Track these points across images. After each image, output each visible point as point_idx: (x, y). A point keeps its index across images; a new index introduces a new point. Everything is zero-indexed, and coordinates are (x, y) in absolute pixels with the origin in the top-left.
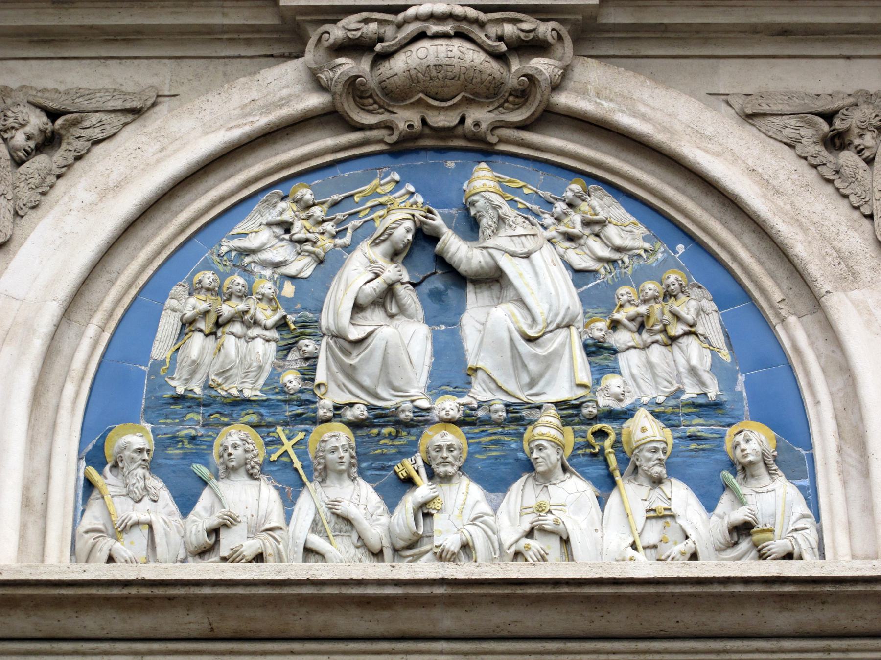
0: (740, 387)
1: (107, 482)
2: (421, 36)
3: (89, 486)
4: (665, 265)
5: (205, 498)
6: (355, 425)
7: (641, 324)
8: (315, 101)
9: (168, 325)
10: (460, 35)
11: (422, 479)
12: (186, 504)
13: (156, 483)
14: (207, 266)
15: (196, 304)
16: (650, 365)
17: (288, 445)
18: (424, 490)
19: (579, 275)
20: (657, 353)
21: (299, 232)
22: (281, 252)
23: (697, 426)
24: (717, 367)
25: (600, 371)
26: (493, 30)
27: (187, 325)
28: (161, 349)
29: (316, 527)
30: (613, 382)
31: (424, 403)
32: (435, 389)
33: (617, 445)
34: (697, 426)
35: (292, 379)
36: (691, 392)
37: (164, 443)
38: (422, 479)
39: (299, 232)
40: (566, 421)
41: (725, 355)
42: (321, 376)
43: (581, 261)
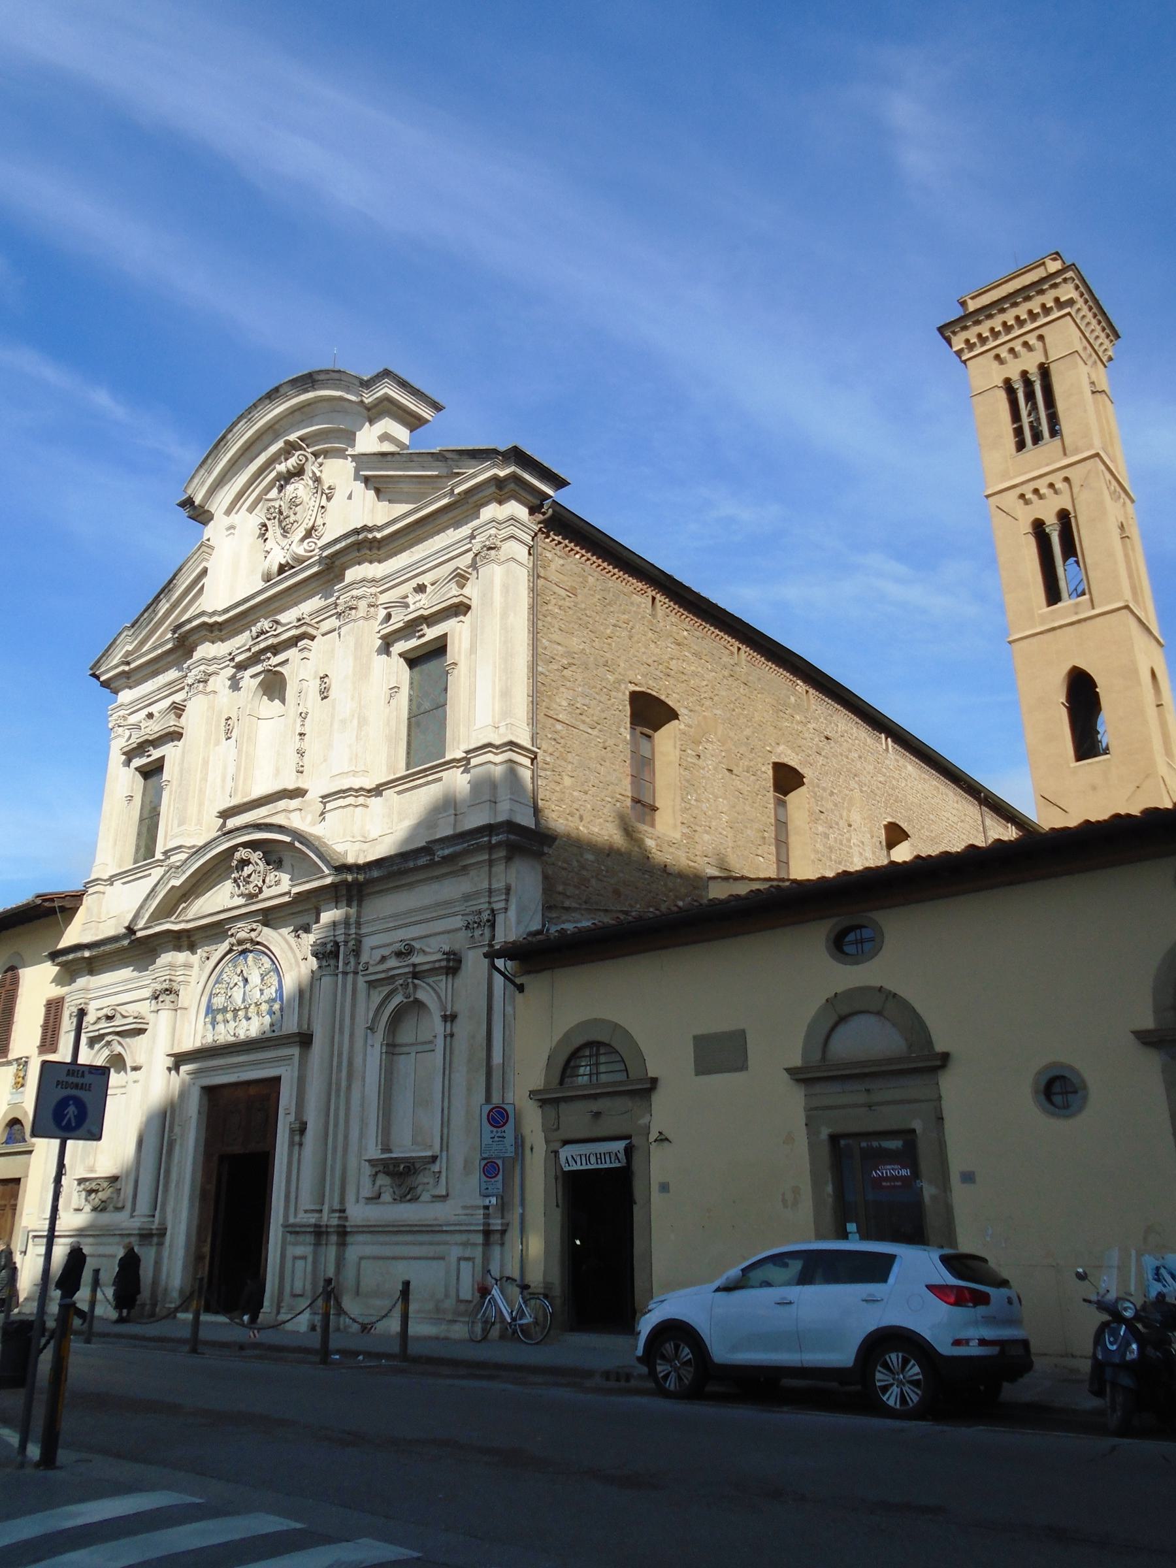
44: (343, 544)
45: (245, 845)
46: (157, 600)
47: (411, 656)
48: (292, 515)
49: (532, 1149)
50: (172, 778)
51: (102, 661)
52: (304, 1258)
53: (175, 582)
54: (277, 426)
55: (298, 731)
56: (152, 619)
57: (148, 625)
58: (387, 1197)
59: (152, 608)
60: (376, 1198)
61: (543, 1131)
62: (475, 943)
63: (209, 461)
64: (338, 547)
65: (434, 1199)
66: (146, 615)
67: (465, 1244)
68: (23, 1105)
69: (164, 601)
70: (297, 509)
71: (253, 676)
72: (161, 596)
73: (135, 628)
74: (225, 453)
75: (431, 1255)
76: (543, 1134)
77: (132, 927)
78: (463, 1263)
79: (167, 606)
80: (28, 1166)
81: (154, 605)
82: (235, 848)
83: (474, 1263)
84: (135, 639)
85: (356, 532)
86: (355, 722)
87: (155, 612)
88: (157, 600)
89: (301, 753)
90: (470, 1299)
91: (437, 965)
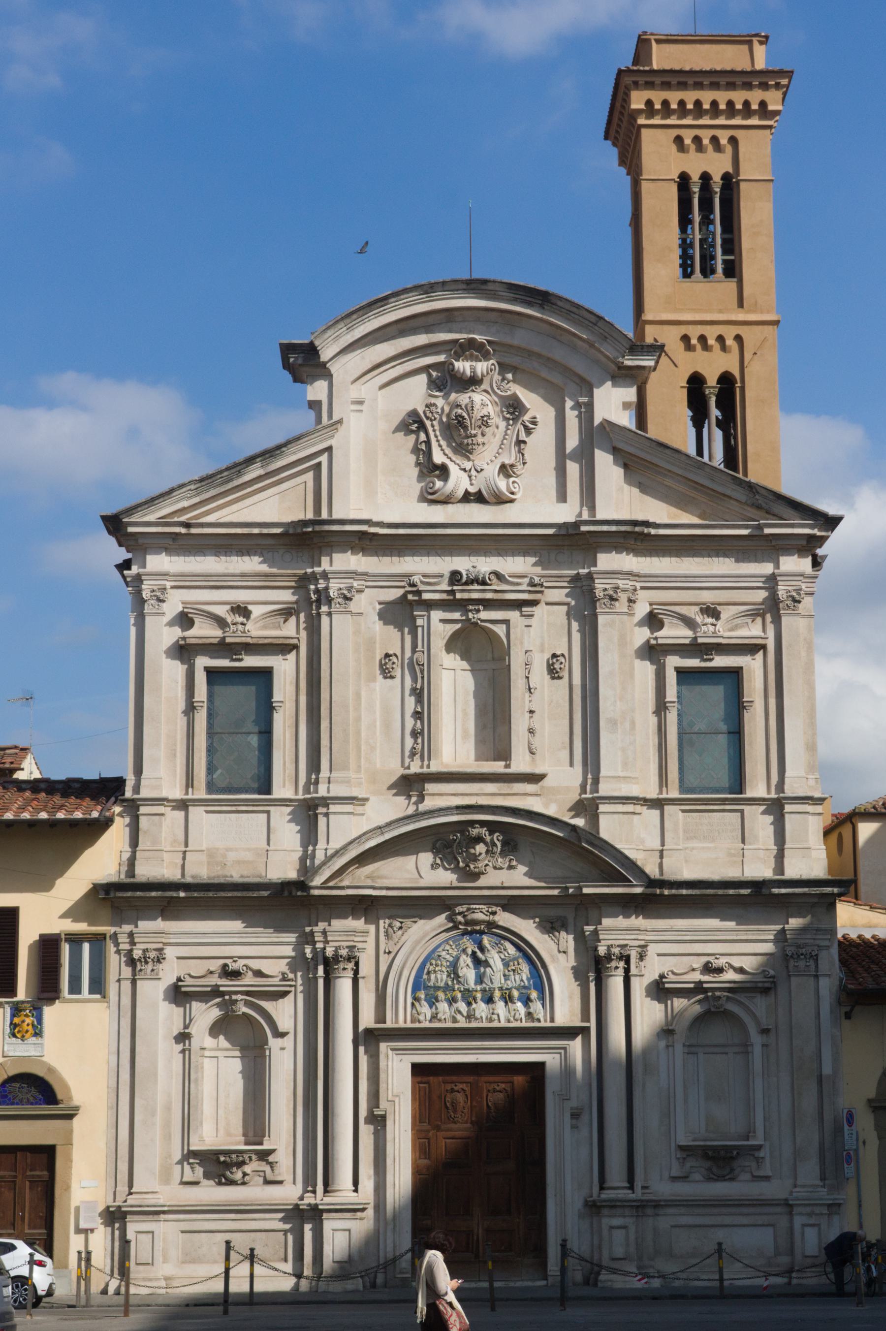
0: (531, 983)
1: (417, 1004)
2: (473, 912)
3: (413, 1004)
4: (518, 957)
5: (434, 1007)
6: (460, 991)
7: (514, 971)
8: (451, 925)
9: (426, 971)
10: (481, 912)
11: (473, 1003)
12: (431, 1007)
13: (425, 1004)
14: (433, 959)
15: (431, 968)
16: (515, 979)
17: (449, 995)
18: (474, 1006)
19: (503, 960)
20: (517, 977)
21: (450, 952)
22: (448, 957)
23: (524, 991)
24: (528, 979)
25: (506, 980)
26: (487, 909)
27: (429, 973)
28: (425, 977)
29: (455, 1012)
30: (509, 982)
31: (473, 987)
32: (476, 984)
33: (509, 996)
34: (524, 991)
35: (450, 983)
36: (522, 984)
37: (426, 995)
38: (473, 1003)
39: (450, 952)
40: (499, 990)
41: (529, 976)
42: (455, 982)
43: (503, 957)
44: (614, 528)
45: (483, 823)
46: (250, 461)
47: (679, 670)
48: (479, 435)
49: (864, 1143)
50: (285, 697)
51: (139, 509)
52: (624, 1227)
53: (284, 449)
54: (456, 313)
55: (527, 709)
56: (231, 480)
57: (222, 484)
58: (697, 1176)
59: (238, 468)
60: (684, 1178)
61: (876, 1129)
62: (799, 972)
63: (354, 316)
64: (605, 528)
65: (755, 1179)
66: (226, 474)
67: (810, 1215)
68: (44, 1059)
69: (259, 464)
70: (487, 430)
71: (444, 621)
72: (258, 460)
73: (203, 483)
74: (380, 315)
75: (760, 1222)
76: (875, 1133)
77: (306, 883)
78: (808, 1230)
79: (261, 472)
80: (71, 1132)
81: (244, 465)
82: (472, 823)
83: (820, 1229)
84: (195, 496)
85: (635, 523)
86: (627, 725)
87: (239, 474)
88: (250, 461)
89: (531, 731)
90: (817, 1254)
91: (760, 985)
